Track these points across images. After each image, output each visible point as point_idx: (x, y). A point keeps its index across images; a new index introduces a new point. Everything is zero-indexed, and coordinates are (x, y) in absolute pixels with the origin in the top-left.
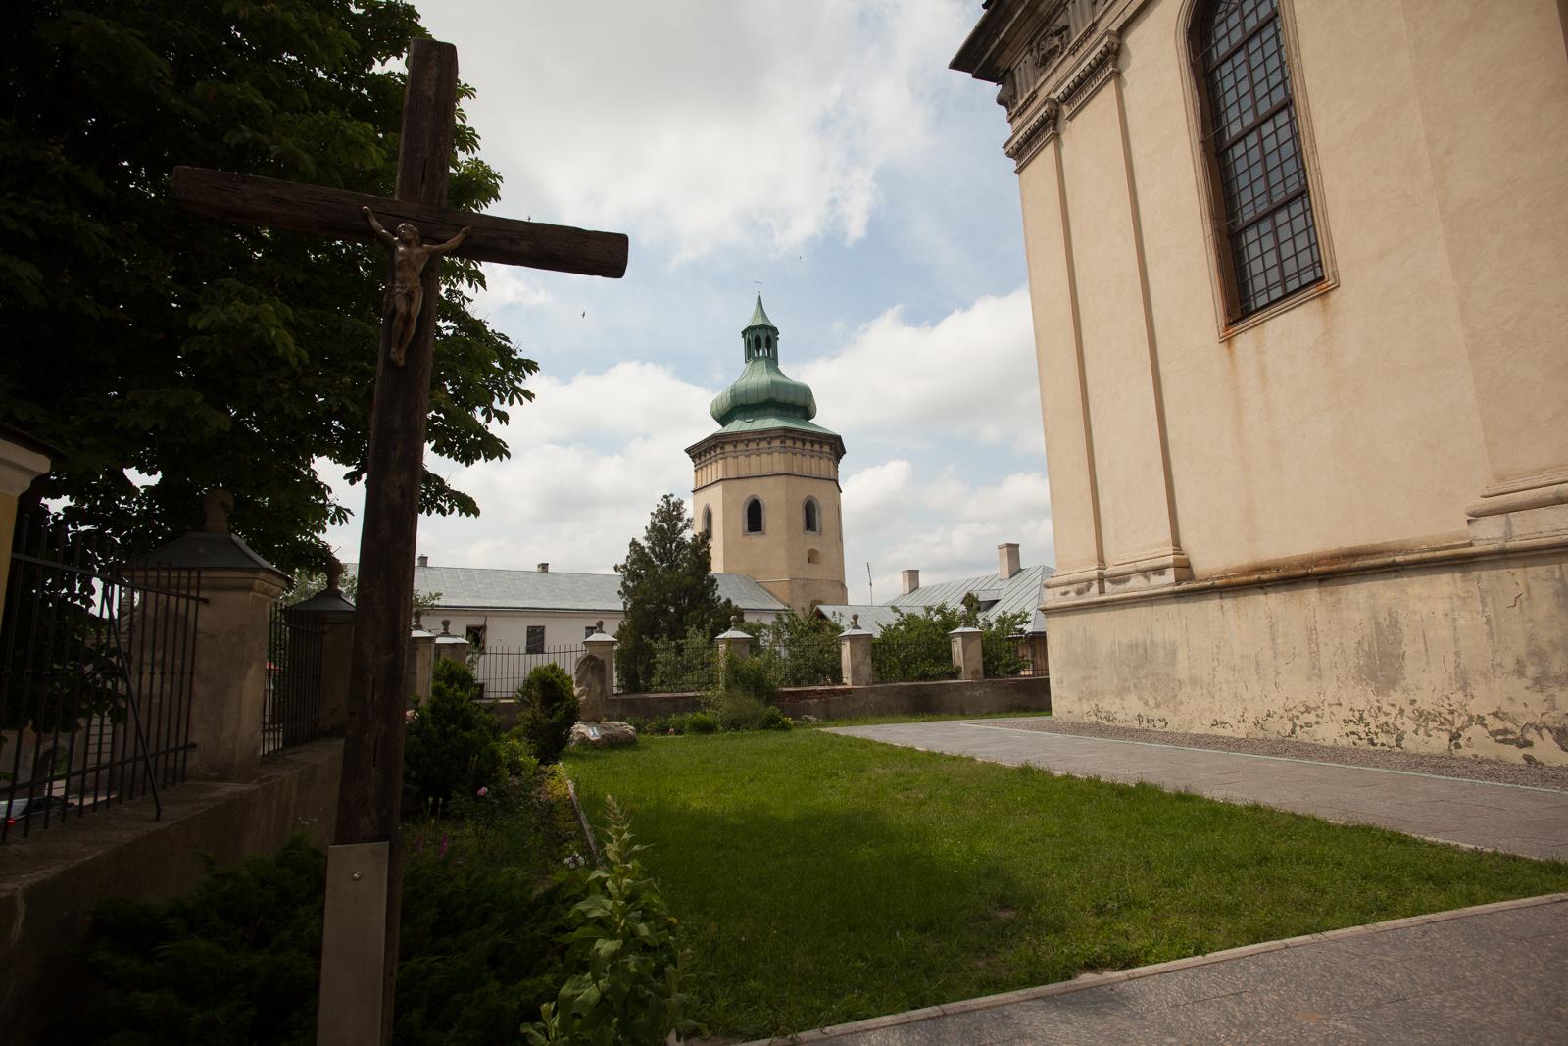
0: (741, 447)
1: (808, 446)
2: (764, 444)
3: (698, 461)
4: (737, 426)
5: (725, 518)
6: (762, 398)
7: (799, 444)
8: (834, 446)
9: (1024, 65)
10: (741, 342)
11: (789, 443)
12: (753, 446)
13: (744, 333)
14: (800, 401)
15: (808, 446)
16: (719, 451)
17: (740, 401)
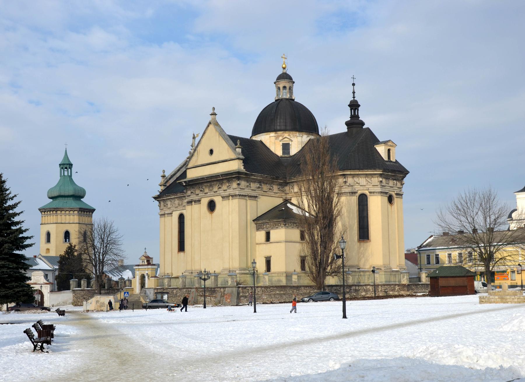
0: (63, 212)
1: (85, 213)
2: (72, 212)
3: (43, 213)
4: (59, 203)
5: (57, 237)
6: (71, 193)
7: (83, 213)
8: (93, 210)
9: (162, 203)
10: (59, 169)
11: (80, 212)
12: (67, 212)
13: (60, 165)
14: (82, 195)
15: (85, 213)
16: (54, 212)
17: (63, 194)
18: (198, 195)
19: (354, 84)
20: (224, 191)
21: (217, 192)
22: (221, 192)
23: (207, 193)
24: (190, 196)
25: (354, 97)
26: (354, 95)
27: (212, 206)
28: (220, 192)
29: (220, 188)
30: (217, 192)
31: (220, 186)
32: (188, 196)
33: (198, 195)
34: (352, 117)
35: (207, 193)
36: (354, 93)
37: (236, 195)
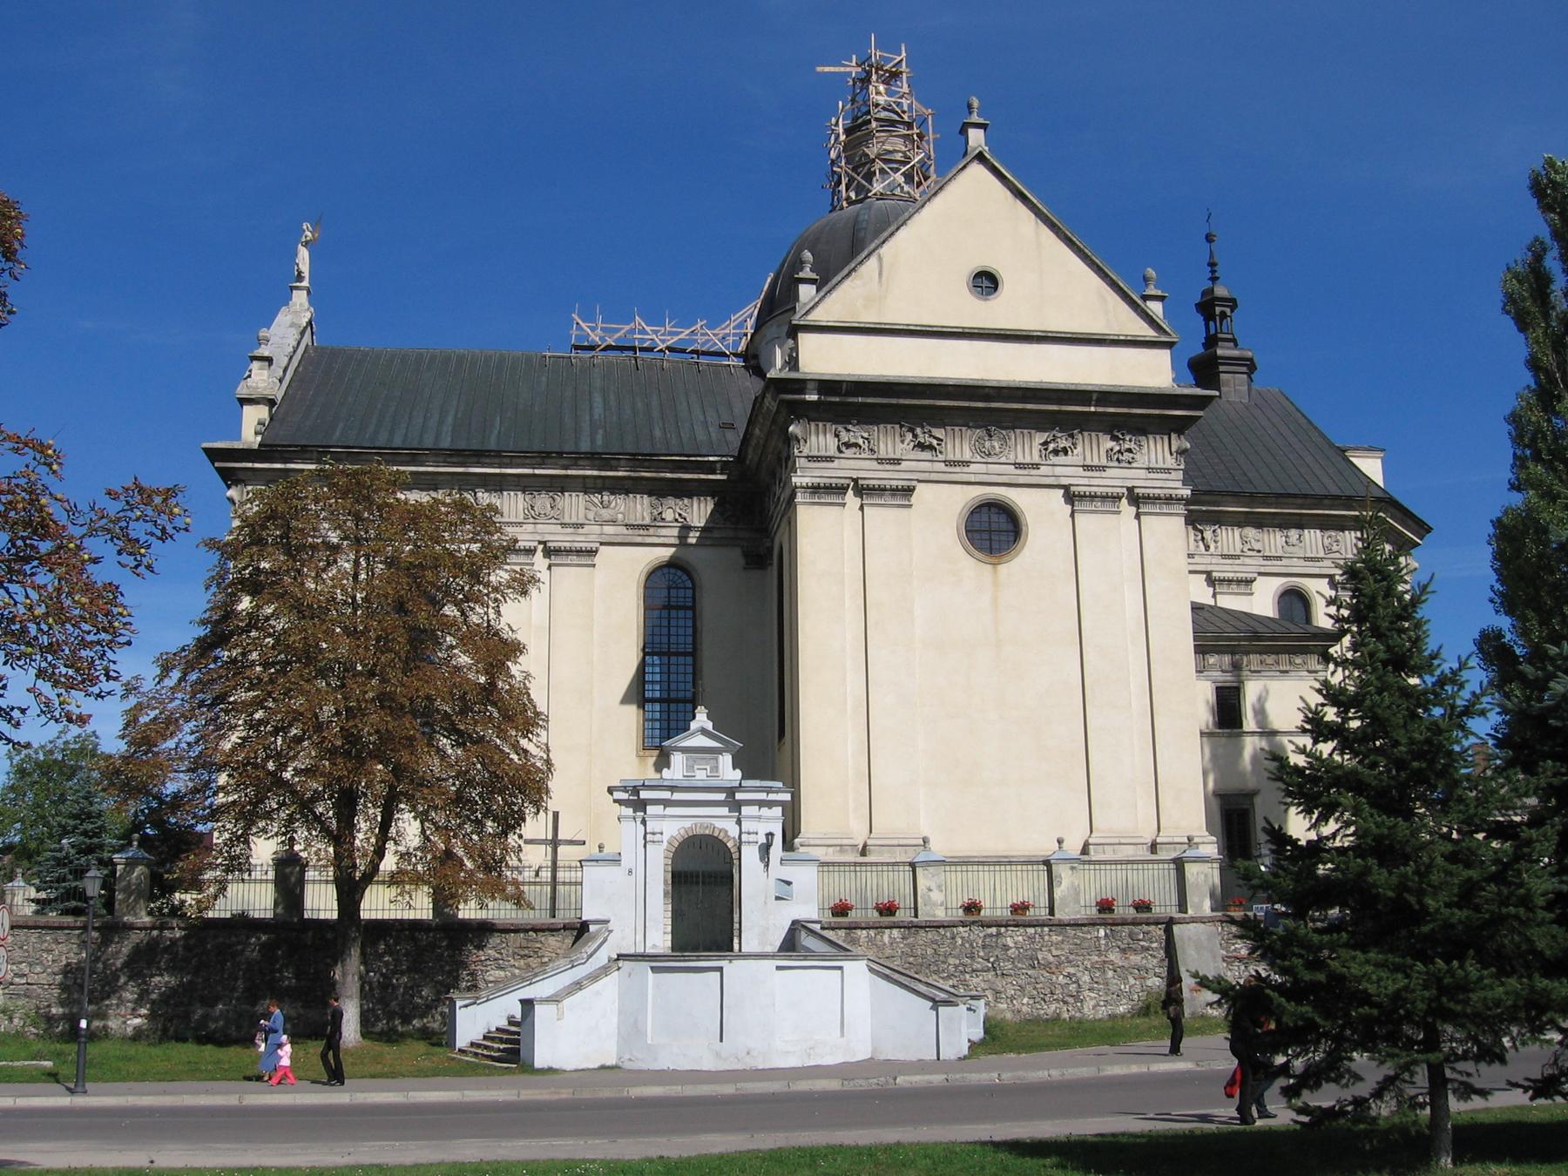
18: (897, 461)
19: (1209, 238)
20: (1087, 468)
21: (1036, 466)
22: (1068, 470)
23: (967, 463)
24: (830, 459)
25: (1214, 279)
26: (1213, 272)
27: (993, 530)
28: (1058, 471)
29: (1065, 451)
30: (1036, 466)
31: (1063, 443)
32: (810, 458)
33: (897, 461)
34: (1211, 341)
35: (967, 463)
36: (1212, 265)
37: (1169, 500)
